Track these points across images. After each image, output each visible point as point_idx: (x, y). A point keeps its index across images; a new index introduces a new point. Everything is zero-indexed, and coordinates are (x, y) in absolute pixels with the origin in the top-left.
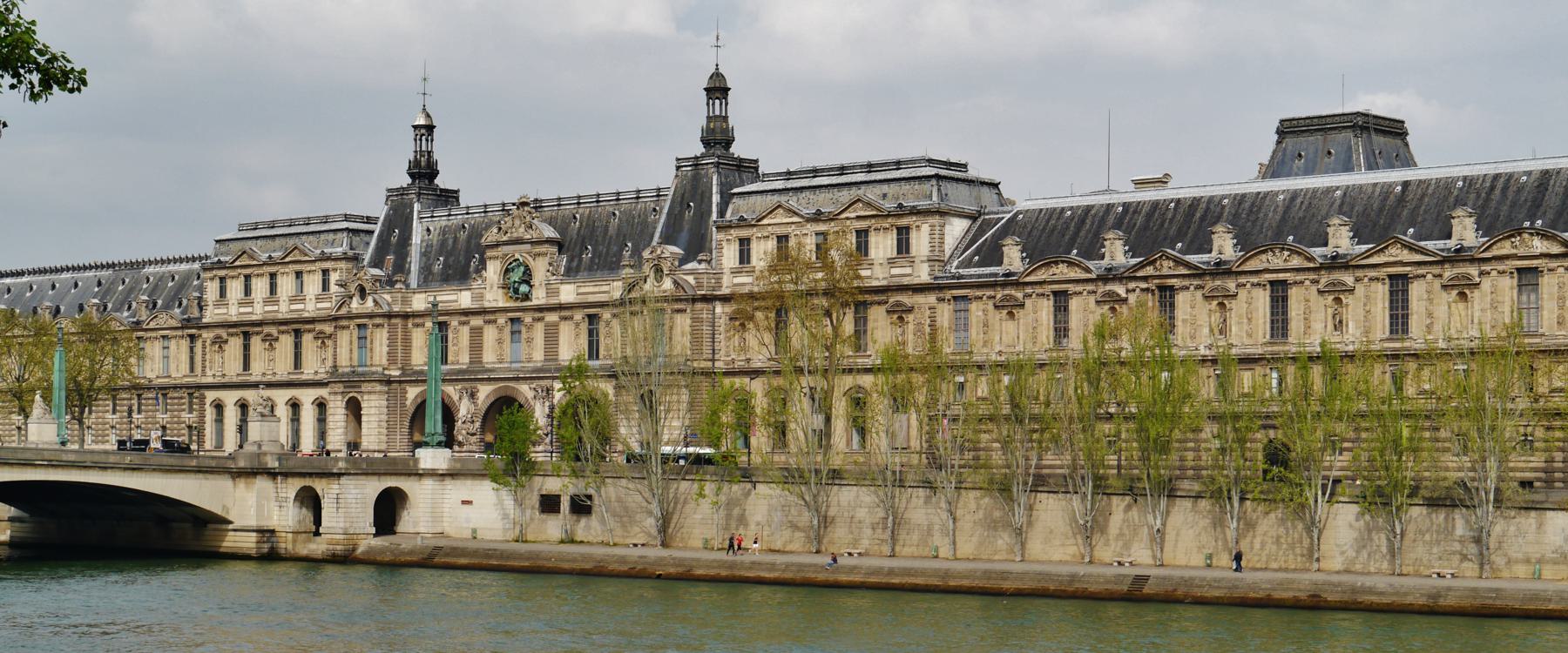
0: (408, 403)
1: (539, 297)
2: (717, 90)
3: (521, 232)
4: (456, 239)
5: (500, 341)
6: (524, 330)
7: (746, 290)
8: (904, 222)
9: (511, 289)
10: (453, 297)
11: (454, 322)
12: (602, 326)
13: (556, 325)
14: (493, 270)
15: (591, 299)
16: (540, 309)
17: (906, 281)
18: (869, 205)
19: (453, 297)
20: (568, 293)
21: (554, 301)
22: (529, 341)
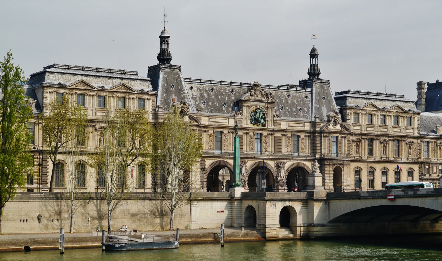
0: (206, 167)
1: (270, 126)
2: (313, 55)
3: (260, 97)
4: (208, 94)
5: (251, 142)
6: (263, 138)
7: (358, 132)
8: (410, 115)
9: (255, 121)
10: (225, 121)
11: (226, 132)
12: (300, 139)
13: (280, 138)
14: (246, 112)
15: (296, 128)
16: (273, 130)
17: (411, 134)
18: (401, 108)
19: (225, 121)
20: (284, 126)
21: (278, 128)
22: (266, 143)
